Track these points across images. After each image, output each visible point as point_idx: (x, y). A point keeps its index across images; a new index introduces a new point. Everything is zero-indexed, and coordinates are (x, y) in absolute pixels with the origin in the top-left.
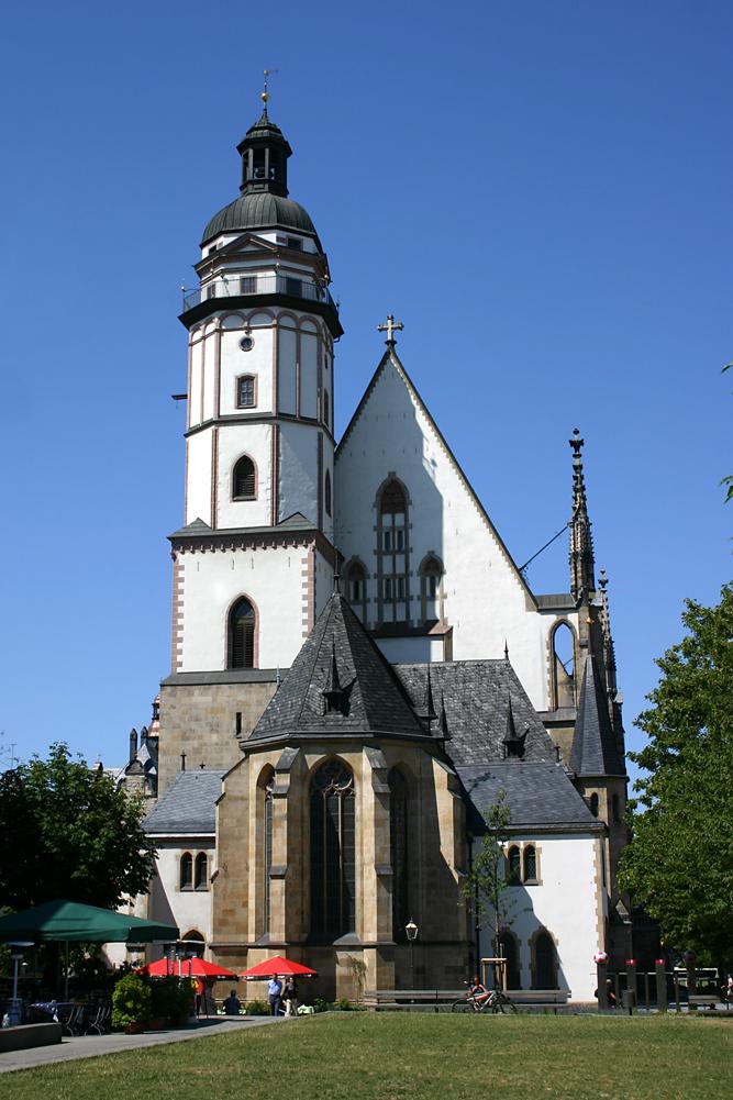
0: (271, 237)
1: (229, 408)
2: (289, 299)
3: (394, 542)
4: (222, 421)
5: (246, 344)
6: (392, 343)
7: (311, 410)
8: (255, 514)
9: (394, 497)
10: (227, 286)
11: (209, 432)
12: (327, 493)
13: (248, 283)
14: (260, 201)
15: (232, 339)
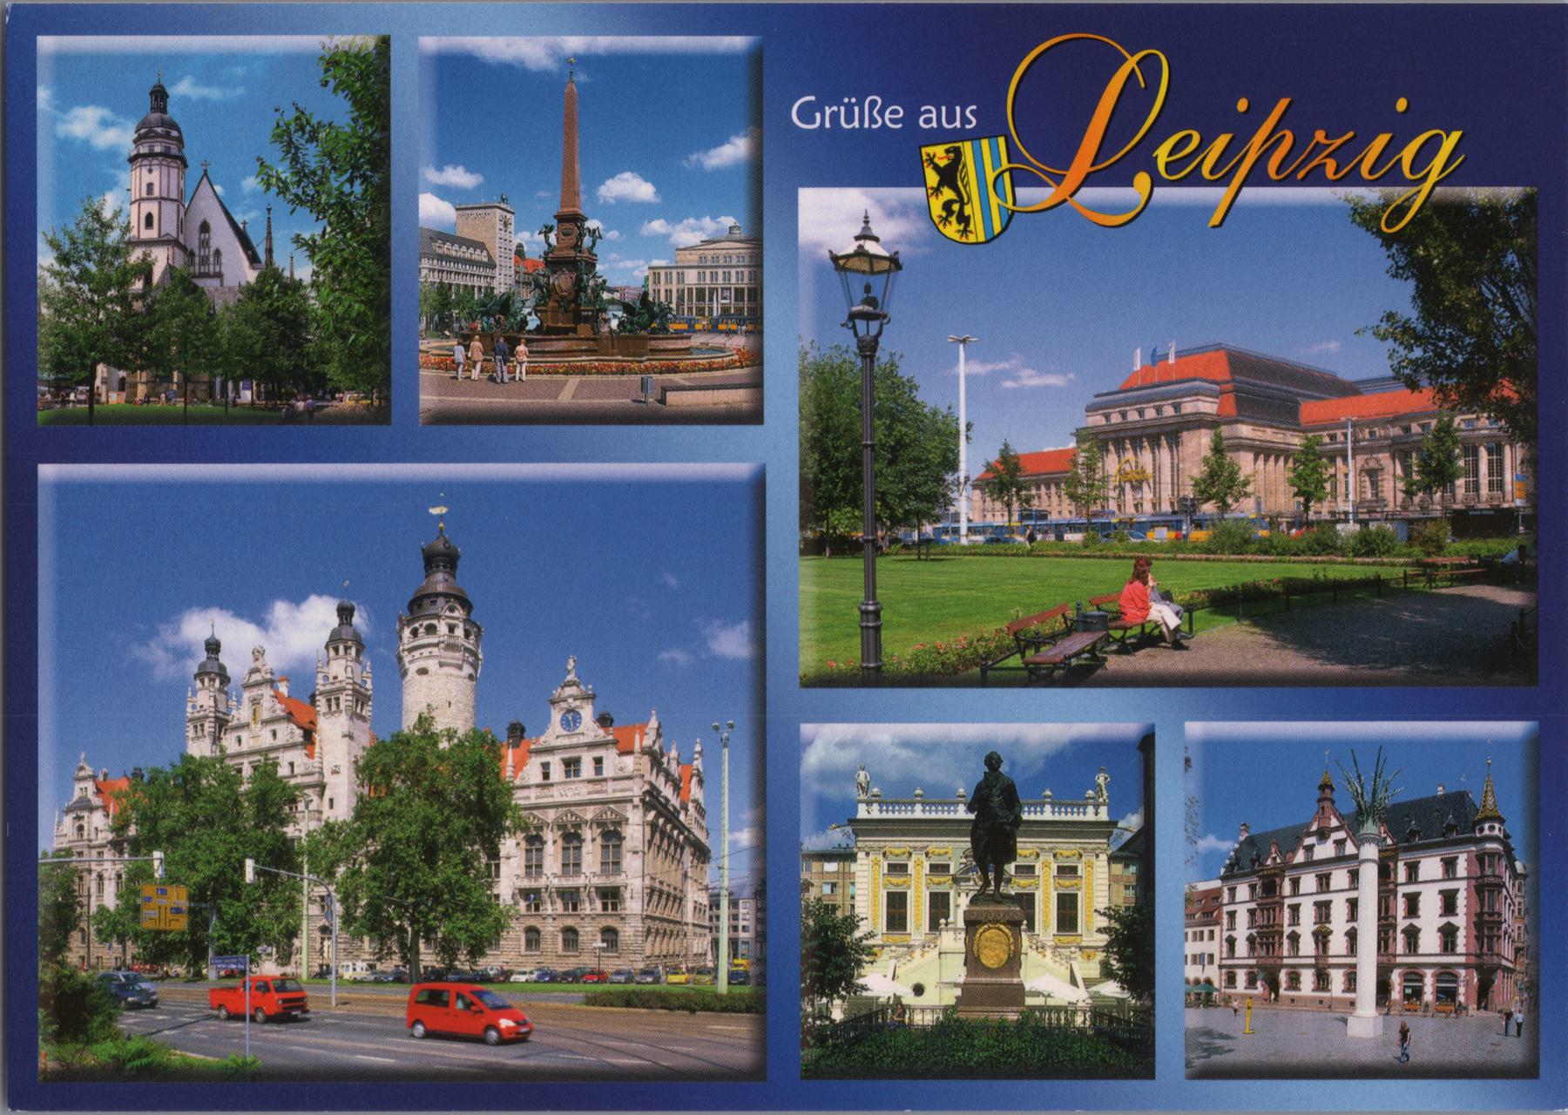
0: (159, 130)
1: (144, 195)
2: (165, 154)
3: (205, 244)
4: (142, 200)
5: (150, 171)
6: (205, 171)
7: (174, 195)
8: (152, 234)
9: (205, 228)
10: (144, 150)
11: (136, 206)
12: (181, 226)
13: (151, 147)
14: (157, 115)
15: (145, 170)
